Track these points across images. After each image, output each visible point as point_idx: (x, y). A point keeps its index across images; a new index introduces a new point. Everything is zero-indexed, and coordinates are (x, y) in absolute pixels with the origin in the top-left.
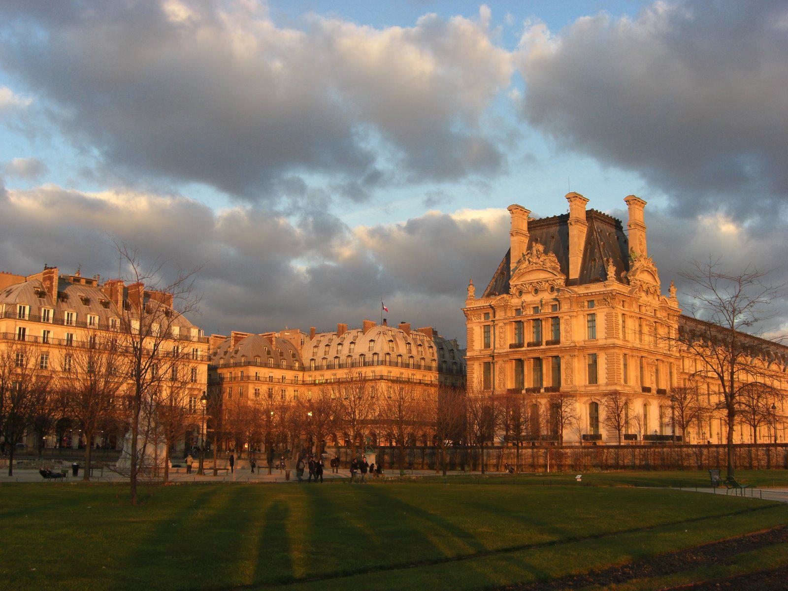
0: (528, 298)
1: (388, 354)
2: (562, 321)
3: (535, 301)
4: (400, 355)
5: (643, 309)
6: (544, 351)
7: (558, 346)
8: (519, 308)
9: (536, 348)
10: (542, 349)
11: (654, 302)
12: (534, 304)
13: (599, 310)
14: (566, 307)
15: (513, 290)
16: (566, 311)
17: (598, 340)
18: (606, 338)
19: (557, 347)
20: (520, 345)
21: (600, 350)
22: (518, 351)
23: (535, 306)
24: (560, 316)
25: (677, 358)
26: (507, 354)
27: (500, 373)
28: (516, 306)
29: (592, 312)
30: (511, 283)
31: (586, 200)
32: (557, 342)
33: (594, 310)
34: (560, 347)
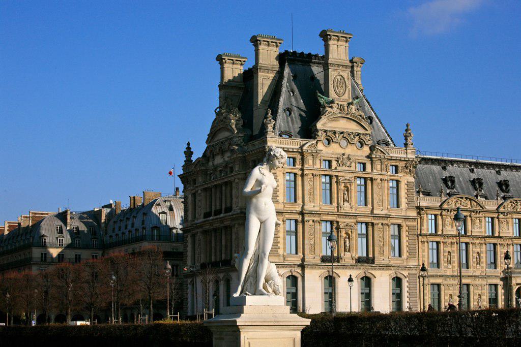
2: (234, 185)
5: (334, 164)
6: (222, 220)
7: (230, 213)
9: (218, 216)
10: (221, 218)
11: (360, 153)
14: (236, 169)
19: (230, 215)
24: (231, 179)
25: (406, 219)
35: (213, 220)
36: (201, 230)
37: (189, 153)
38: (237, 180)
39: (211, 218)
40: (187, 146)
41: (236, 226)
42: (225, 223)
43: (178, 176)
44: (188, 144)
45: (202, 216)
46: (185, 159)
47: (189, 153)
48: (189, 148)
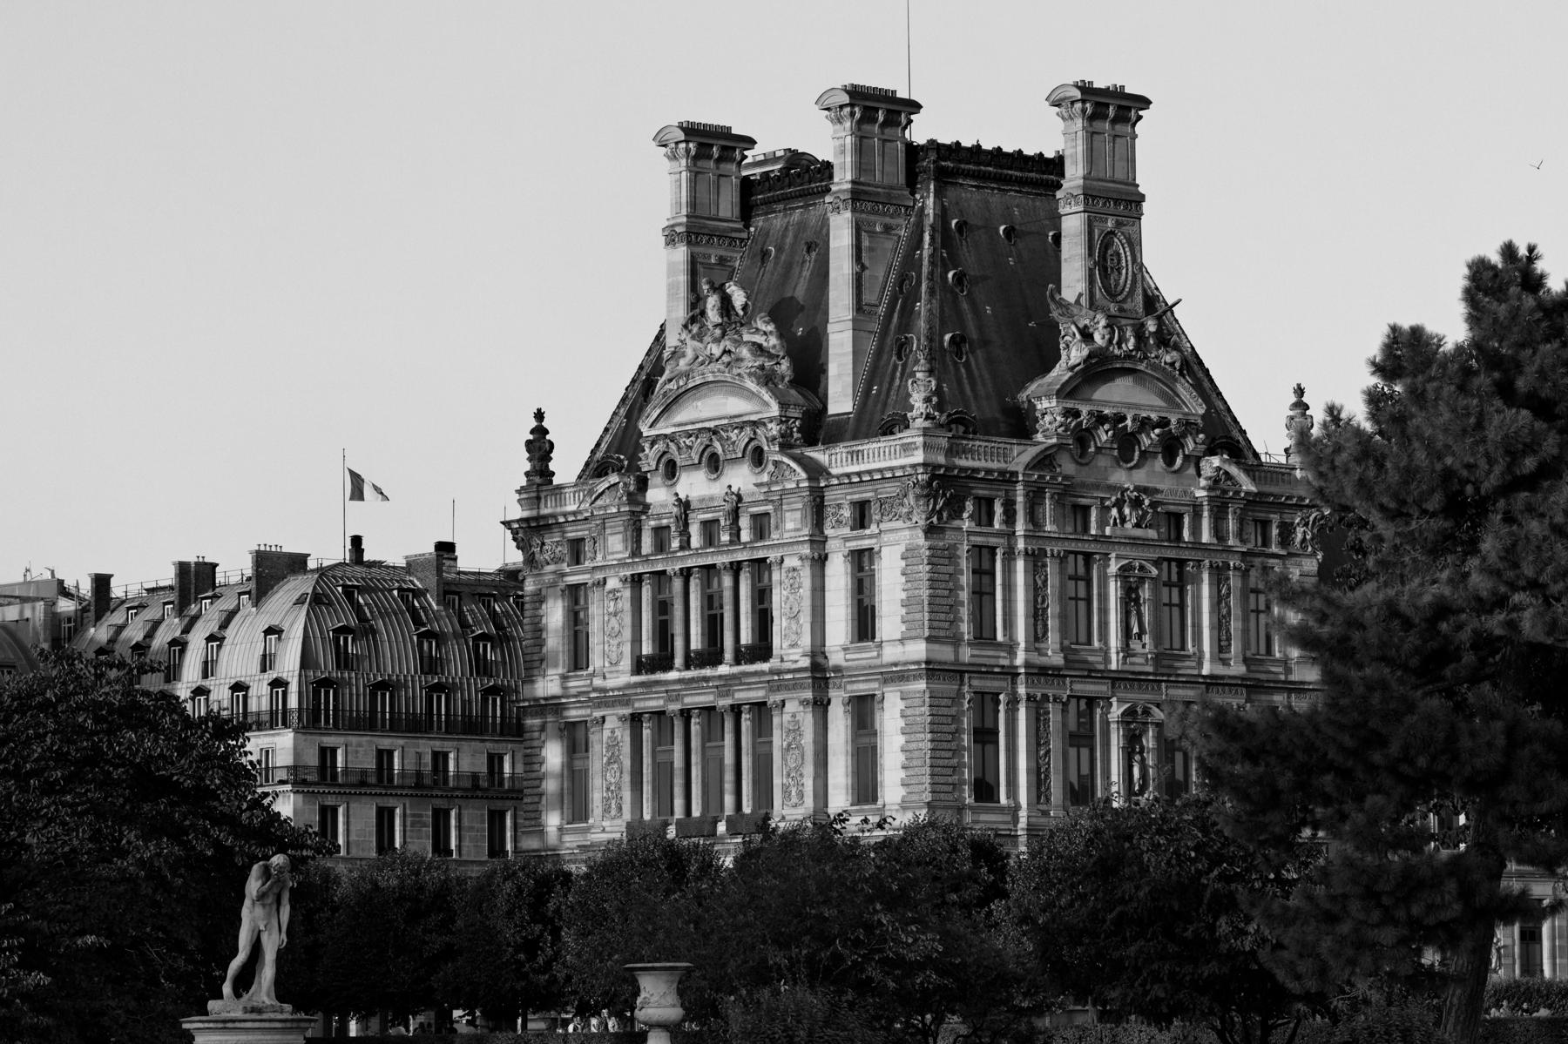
0: (694, 485)
1: (326, 683)
3: (712, 499)
4: (383, 686)
7: (765, 666)
8: (665, 522)
9: (707, 672)
10: (720, 677)
12: (707, 509)
13: (885, 537)
15: (649, 459)
16: (787, 537)
17: (880, 645)
18: (902, 641)
19: (762, 673)
20: (662, 661)
21: (885, 682)
22: (657, 683)
23: (709, 516)
24: (773, 556)
26: (622, 698)
27: (609, 763)
28: (659, 517)
29: (865, 544)
30: (646, 431)
31: (899, 109)
32: (762, 648)
33: (871, 537)
34: (772, 672)
35: (680, 681)
36: (627, 711)
37: (540, 447)
38: (789, 562)
39: (673, 675)
40: (534, 424)
41: (791, 707)
42: (737, 695)
43: (507, 524)
44: (539, 415)
45: (626, 663)
46: (528, 466)
47: (540, 447)
48: (540, 431)
